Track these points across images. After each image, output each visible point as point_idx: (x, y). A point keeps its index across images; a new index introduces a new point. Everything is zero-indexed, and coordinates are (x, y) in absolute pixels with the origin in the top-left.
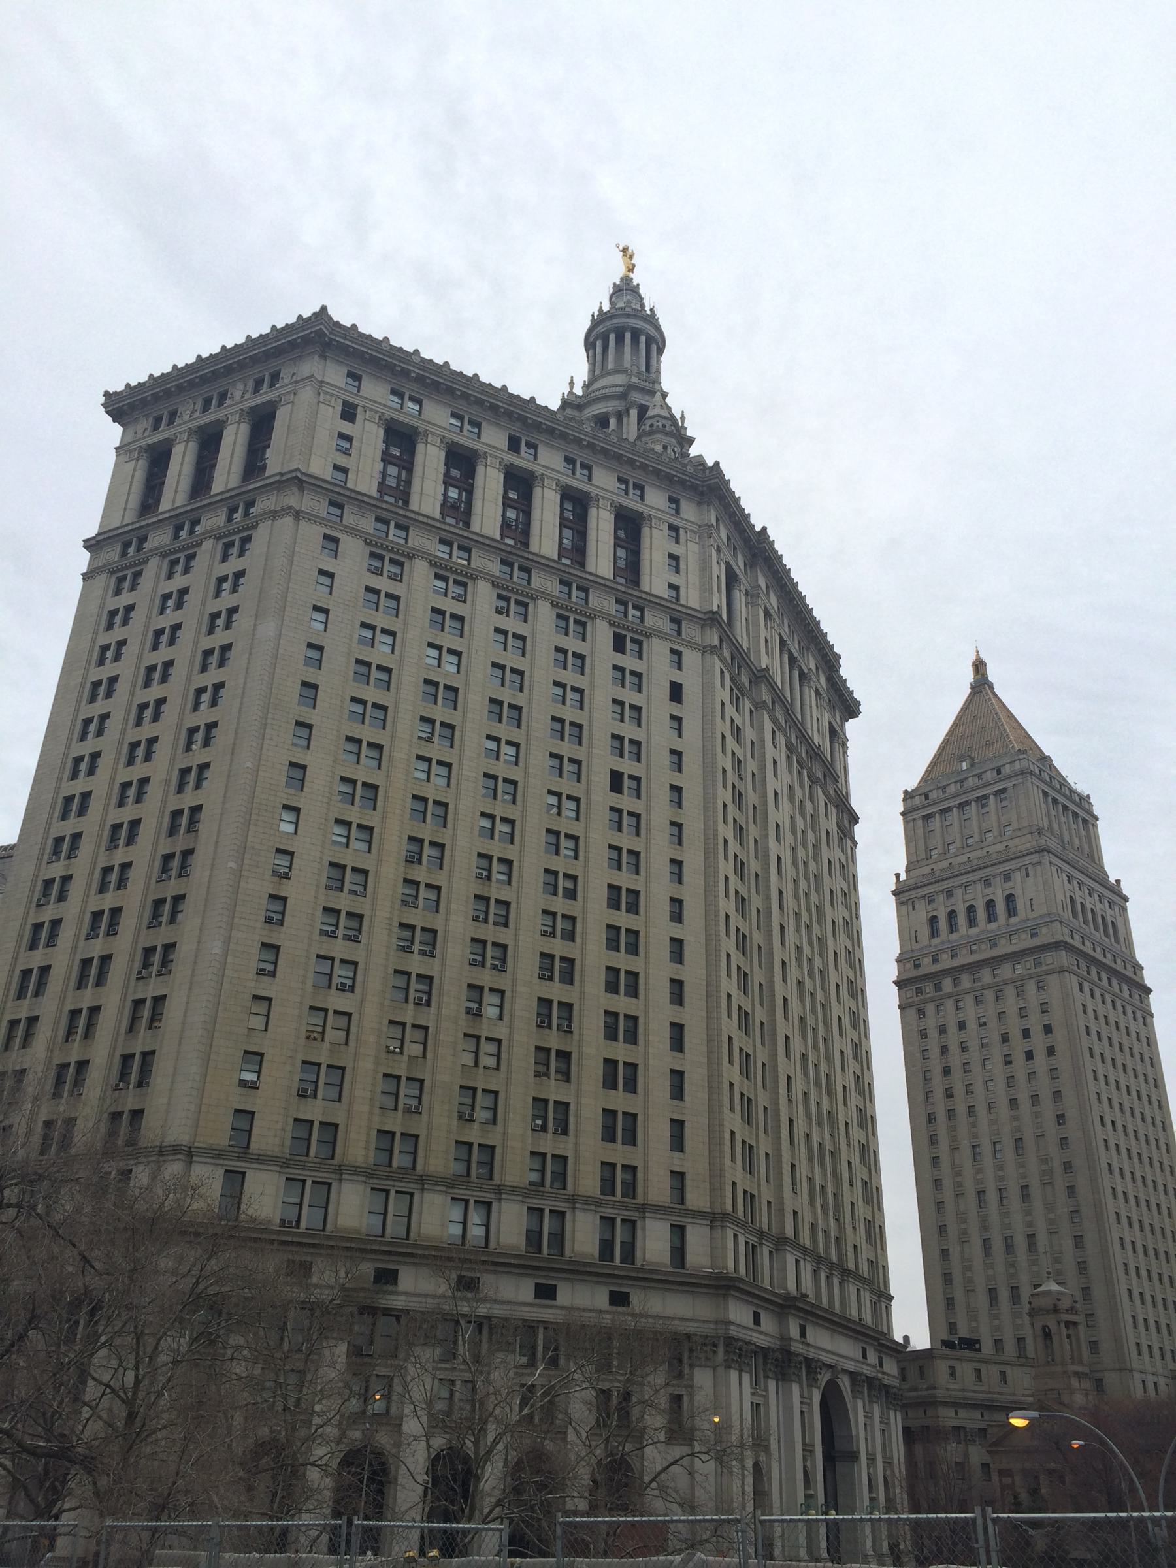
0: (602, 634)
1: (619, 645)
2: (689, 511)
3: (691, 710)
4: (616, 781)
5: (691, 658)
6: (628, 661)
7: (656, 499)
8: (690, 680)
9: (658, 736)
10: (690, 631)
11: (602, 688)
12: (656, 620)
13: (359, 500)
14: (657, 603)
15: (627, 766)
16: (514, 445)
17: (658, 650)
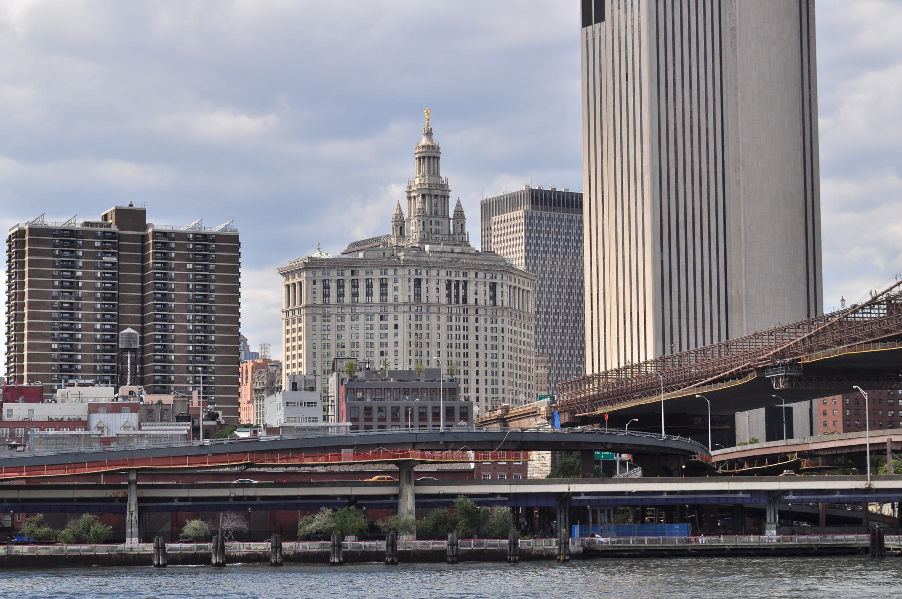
0: (377, 317)
1: (382, 318)
2: (400, 272)
3: (400, 330)
4: (382, 353)
5: (400, 316)
6: (384, 322)
7: (391, 272)
8: (399, 322)
9: (391, 340)
10: (400, 309)
11: (376, 331)
12: (391, 309)
13: (318, 306)
14: (391, 304)
15: (384, 349)
16: (353, 273)
17: (391, 317)
